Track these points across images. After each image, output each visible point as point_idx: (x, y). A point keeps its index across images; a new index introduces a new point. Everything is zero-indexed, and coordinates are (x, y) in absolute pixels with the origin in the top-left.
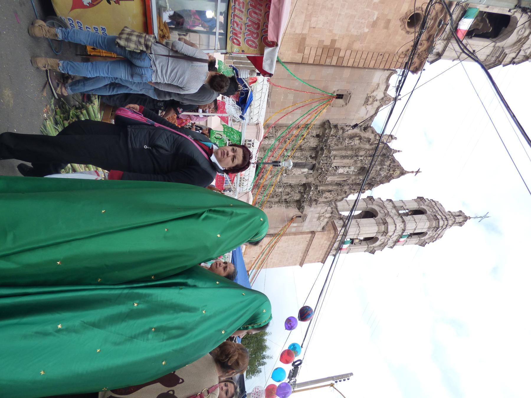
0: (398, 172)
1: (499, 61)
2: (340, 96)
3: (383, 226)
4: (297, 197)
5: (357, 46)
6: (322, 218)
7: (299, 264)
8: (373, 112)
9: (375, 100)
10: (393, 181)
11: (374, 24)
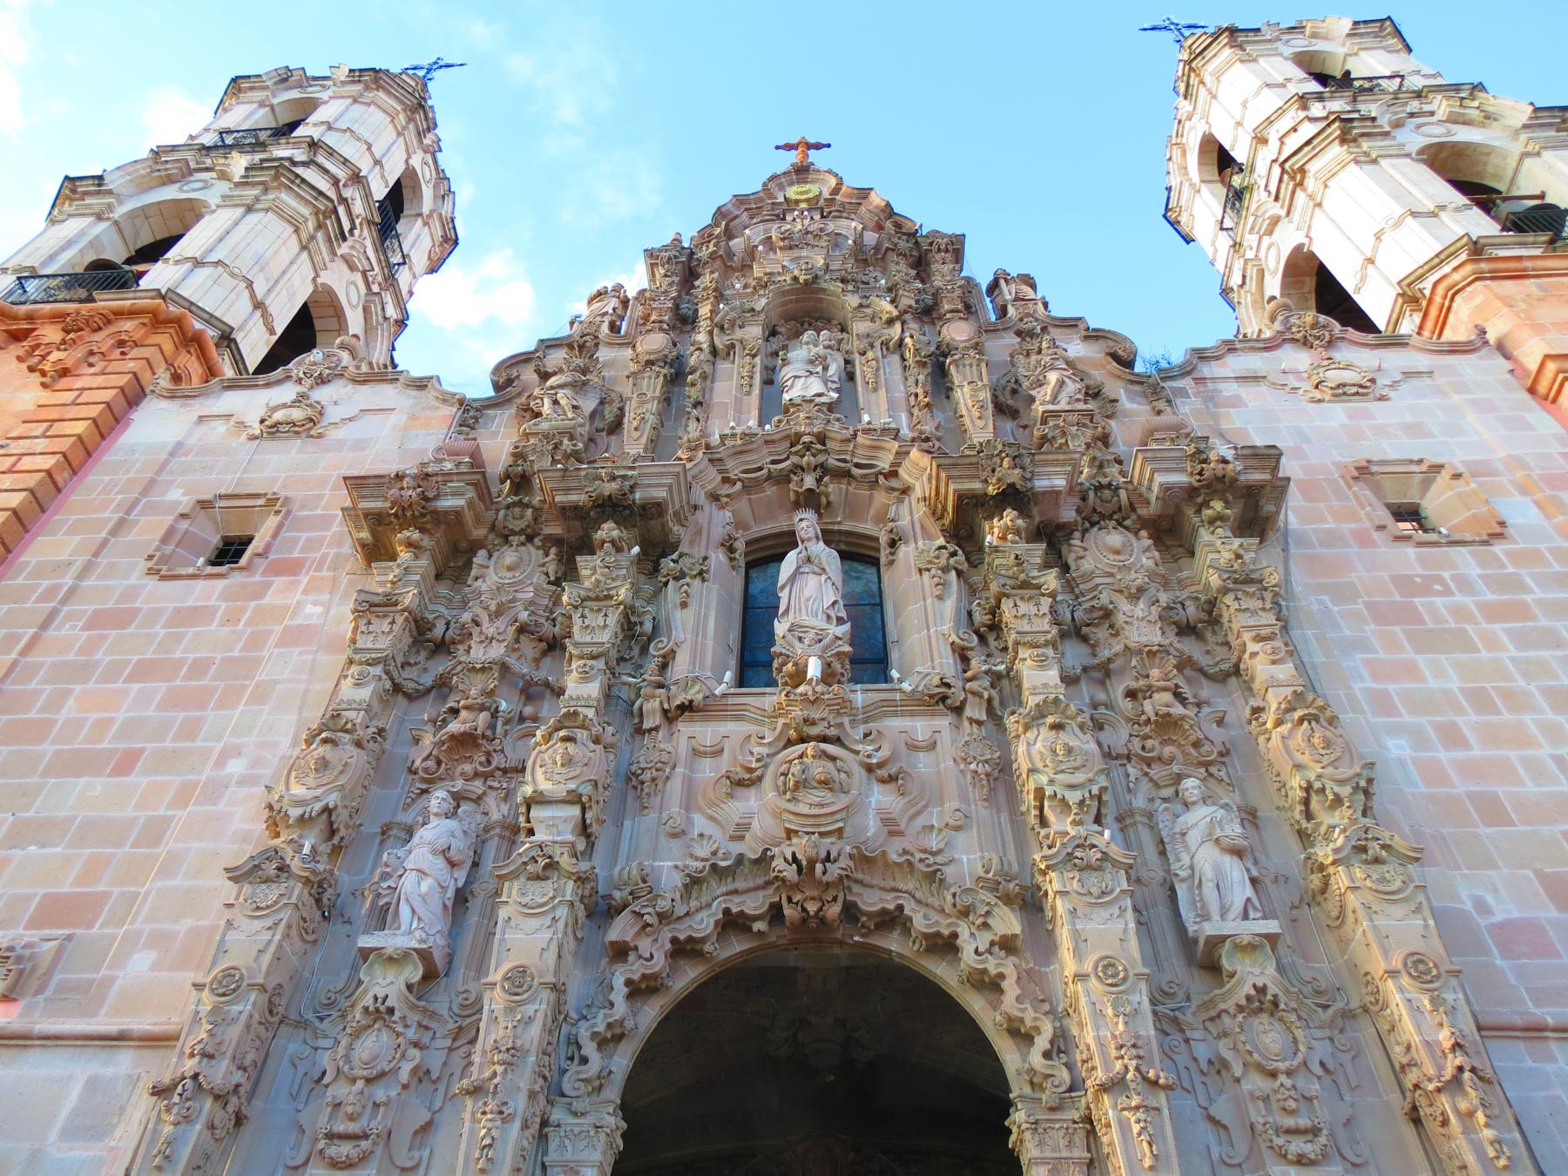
1: (276, 177)
2: (230, 552)
3: (1312, 168)
4: (1112, 555)
6: (1334, 376)
10: (853, 181)
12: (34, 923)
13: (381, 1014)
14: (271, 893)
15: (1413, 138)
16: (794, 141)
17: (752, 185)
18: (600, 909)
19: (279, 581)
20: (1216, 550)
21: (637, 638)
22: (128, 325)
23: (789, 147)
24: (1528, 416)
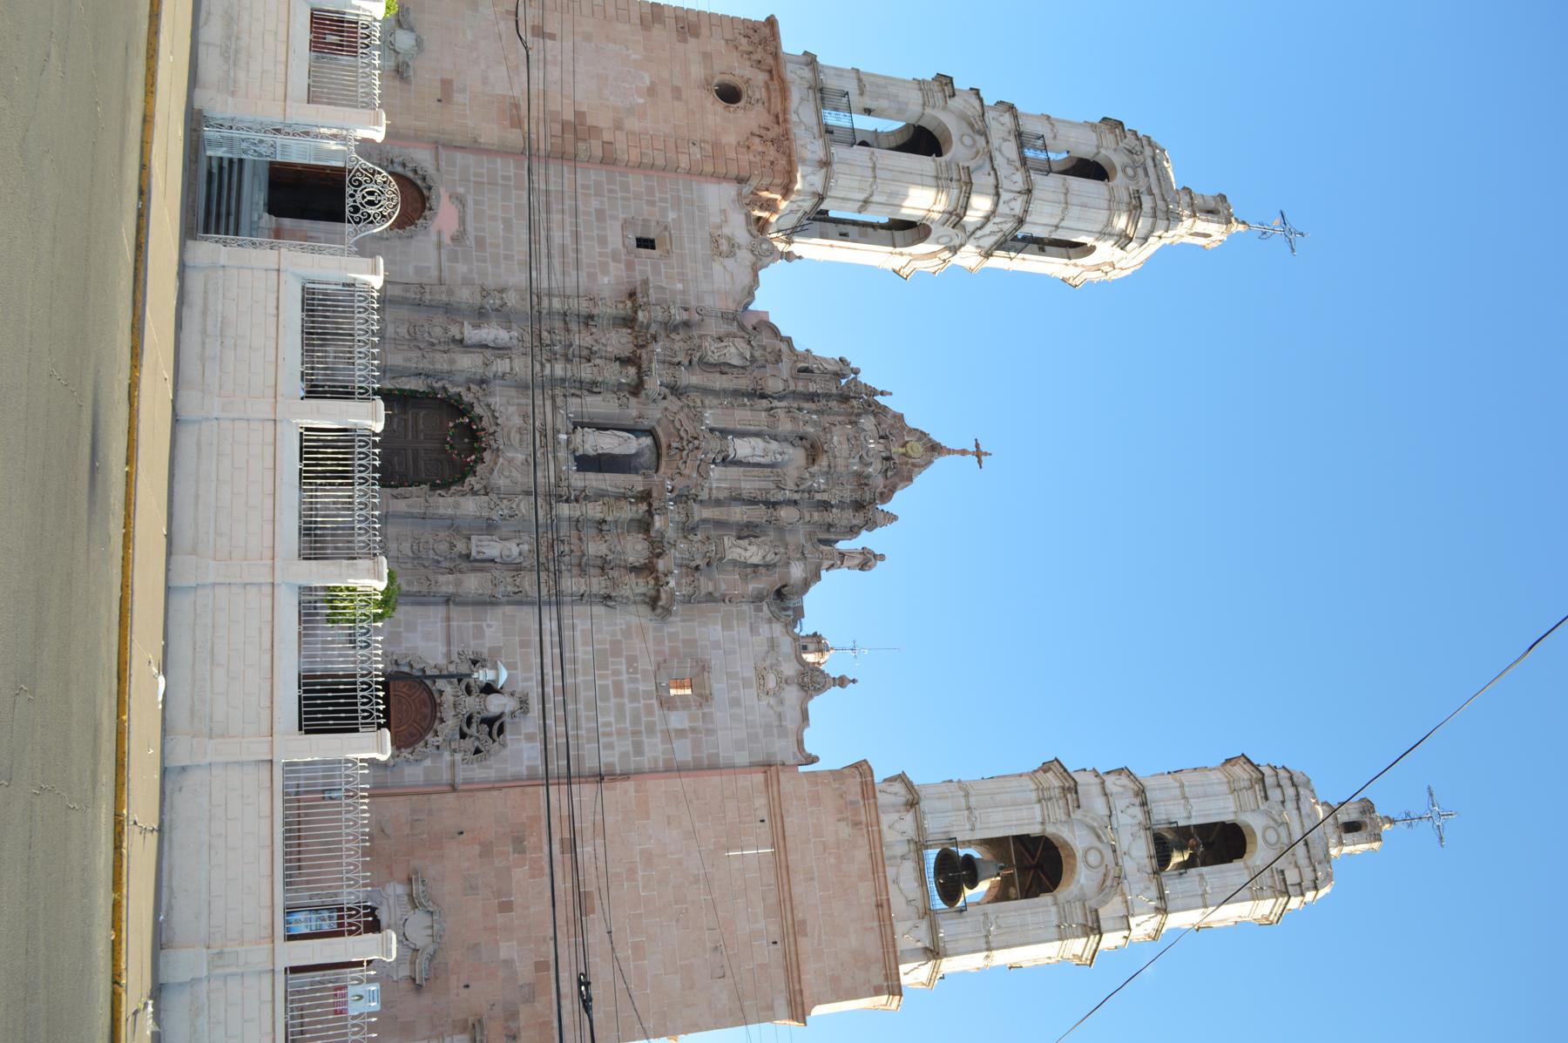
0: (916, 449)
2: (645, 243)
5: (632, 124)
6: (771, 682)
7: (781, 1004)
8: (745, 279)
9: (733, 246)
11: (651, 91)
12: (476, 237)
13: (446, 331)
14: (479, 297)
15: (1076, 838)
16: (983, 449)
17: (911, 422)
18: (482, 382)
19: (622, 266)
20: (638, 586)
21: (592, 388)
22: (783, 162)
23: (977, 446)
24: (746, 753)
